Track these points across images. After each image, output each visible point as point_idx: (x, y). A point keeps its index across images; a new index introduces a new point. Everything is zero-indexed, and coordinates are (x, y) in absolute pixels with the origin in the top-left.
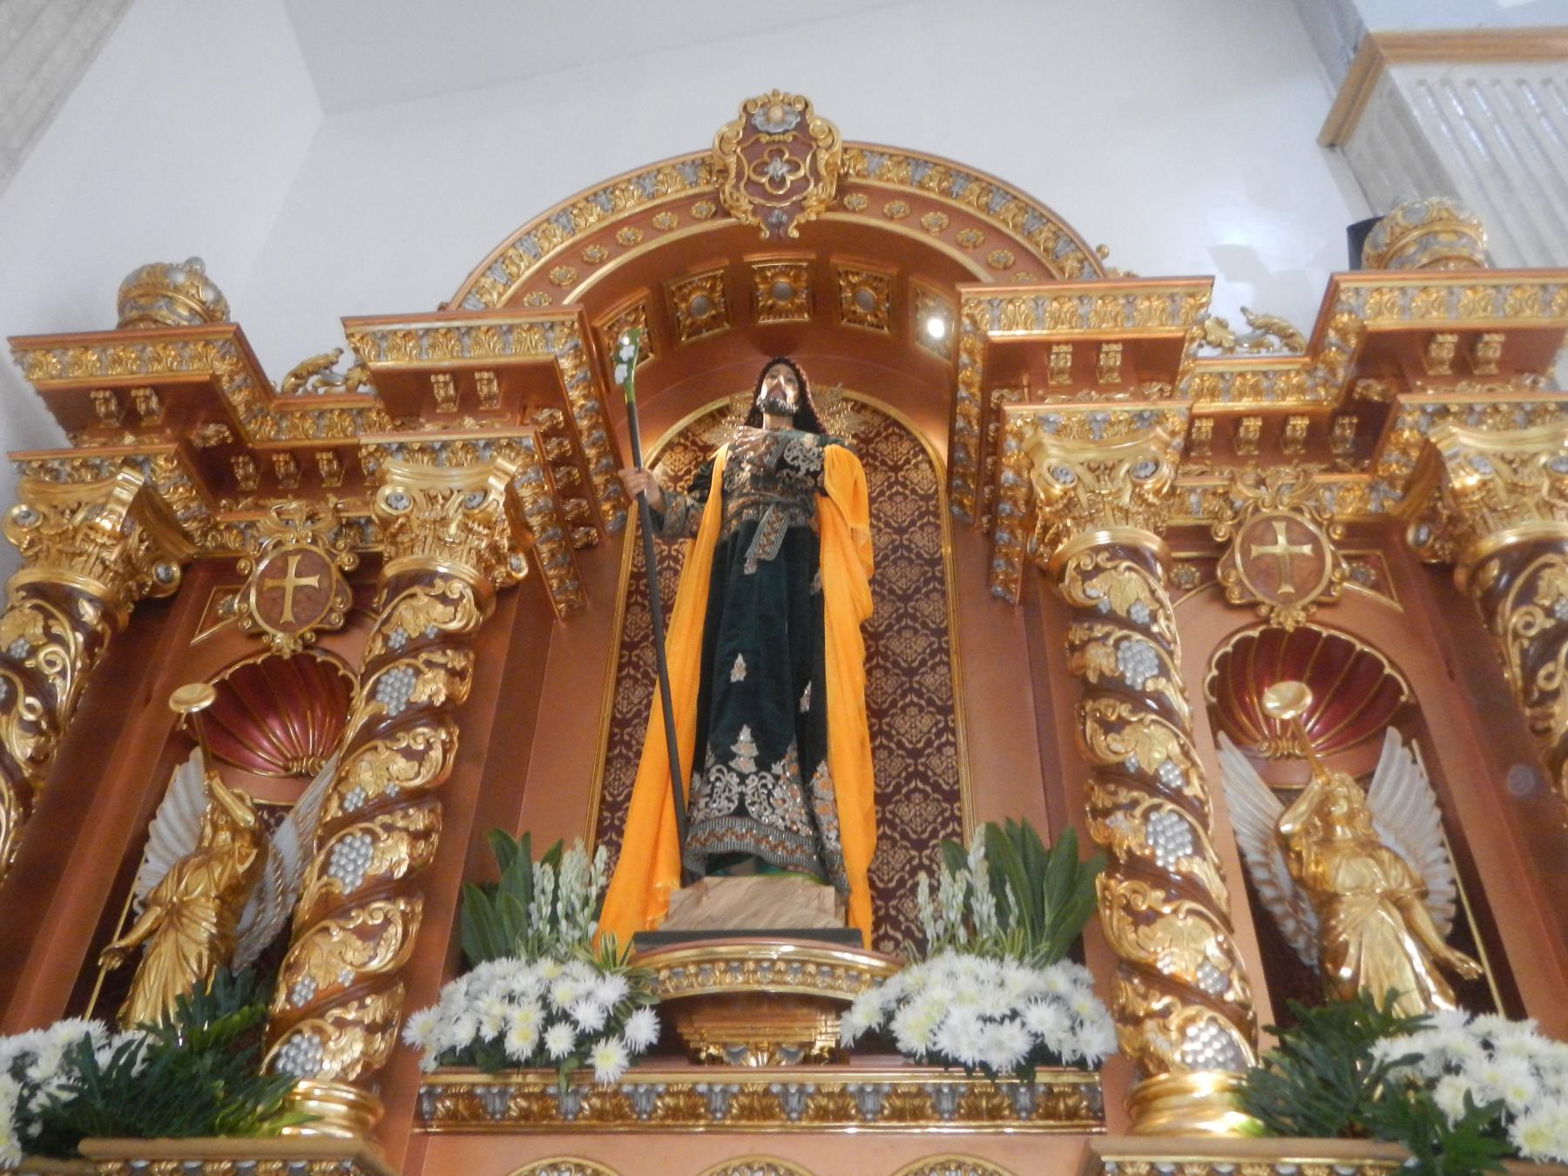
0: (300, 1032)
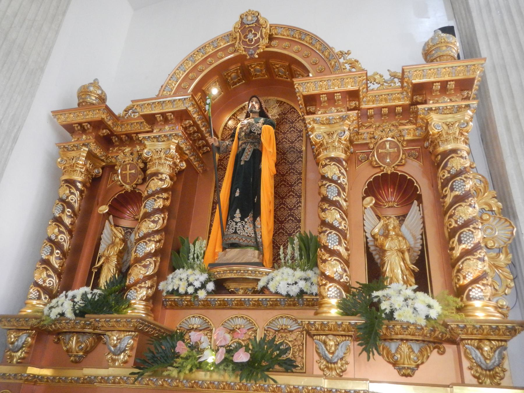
0: (131, 289)
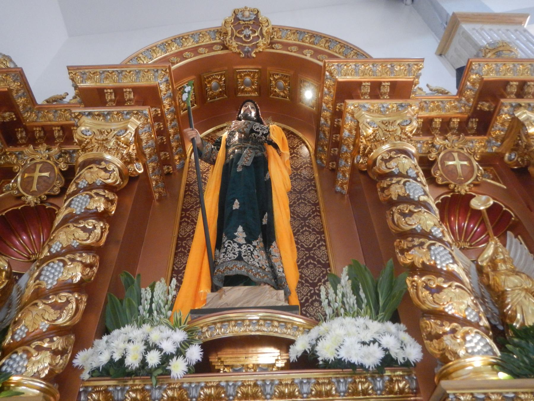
0: (16, 353)
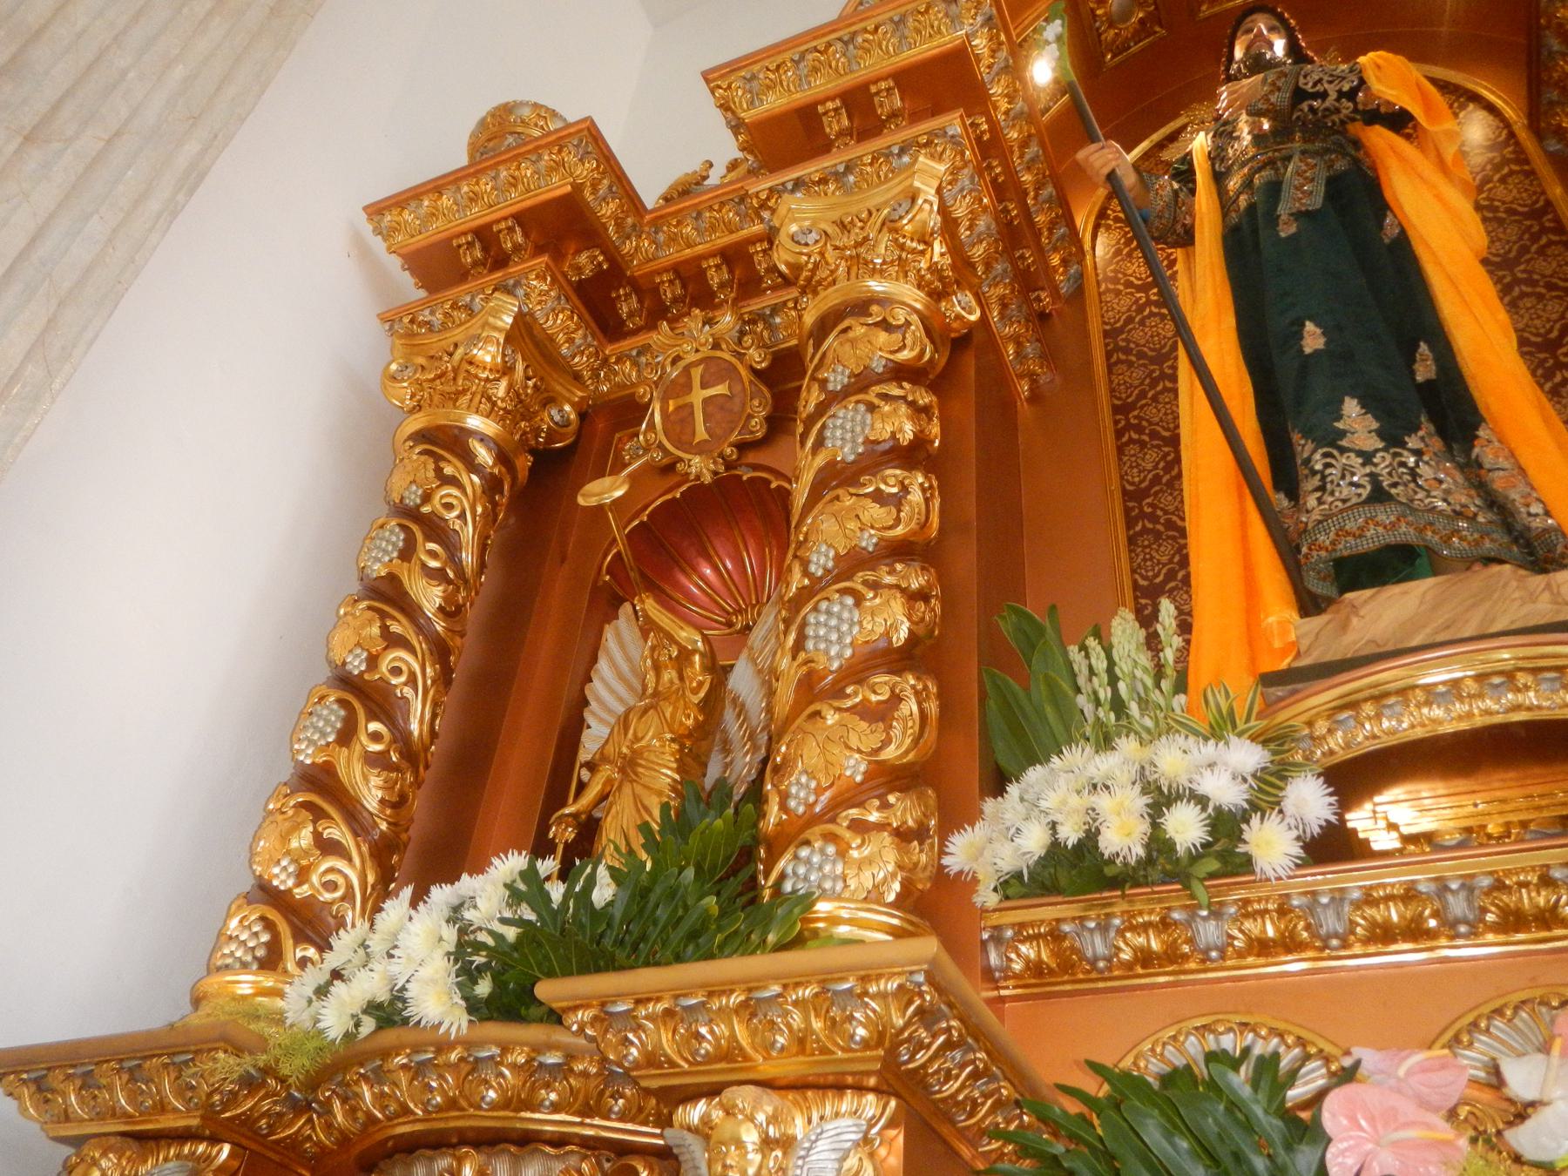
0: (807, 843)
